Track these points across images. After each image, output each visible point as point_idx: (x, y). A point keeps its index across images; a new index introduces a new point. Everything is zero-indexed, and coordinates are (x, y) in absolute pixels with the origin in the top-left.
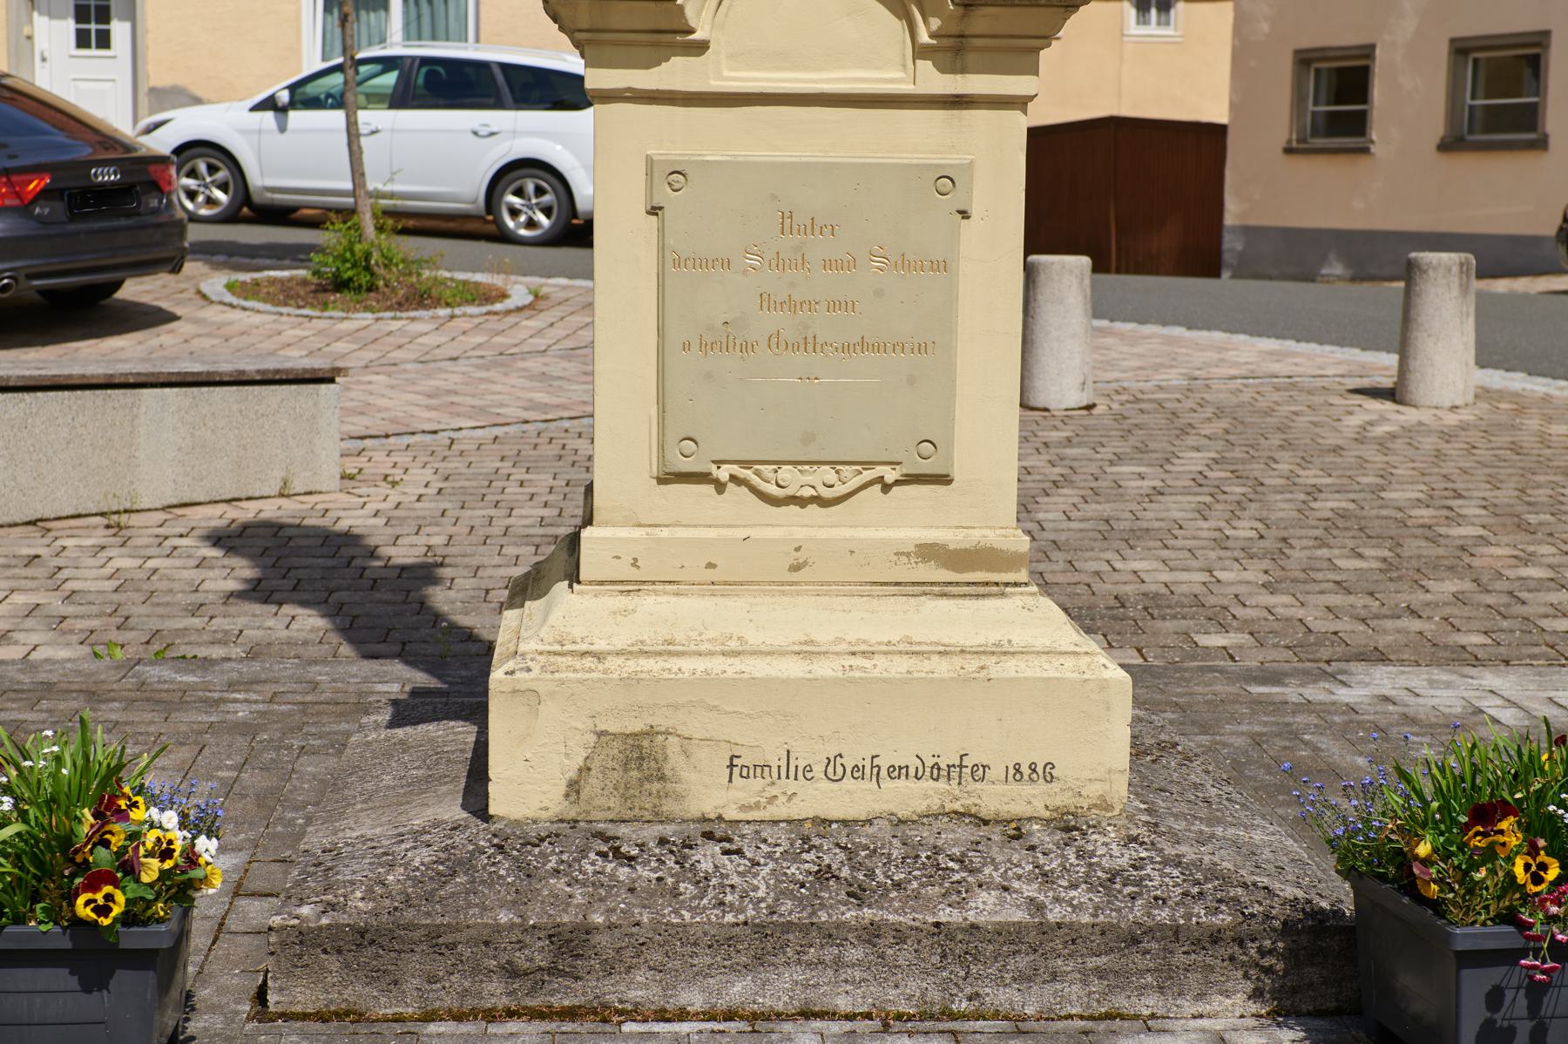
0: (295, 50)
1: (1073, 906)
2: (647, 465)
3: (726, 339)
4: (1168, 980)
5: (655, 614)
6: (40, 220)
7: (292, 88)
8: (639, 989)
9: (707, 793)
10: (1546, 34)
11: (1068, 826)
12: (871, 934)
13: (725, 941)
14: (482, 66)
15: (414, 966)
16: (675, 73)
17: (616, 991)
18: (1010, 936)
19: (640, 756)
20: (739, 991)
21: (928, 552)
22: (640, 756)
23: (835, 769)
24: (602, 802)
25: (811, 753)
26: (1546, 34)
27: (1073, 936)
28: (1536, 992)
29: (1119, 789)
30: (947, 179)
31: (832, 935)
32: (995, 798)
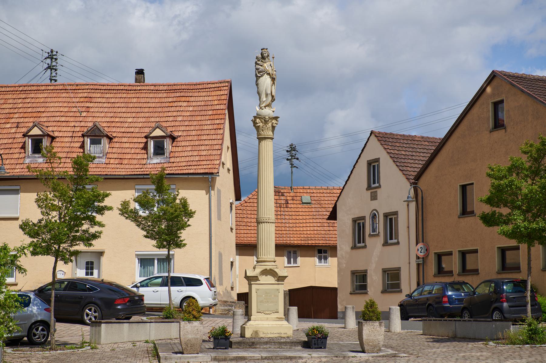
0: (134, 275)
1: (288, 340)
2: (256, 311)
3: (262, 302)
4: (295, 346)
5: (257, 322)
6: (128, 306)
7: (140, 283)
8: (258, 346)
9: (261, 335)
10: (400, 268)
11: (288, 337)
12: (274, 342)
13: (264, 343)
14: (180, 277)
15: (243, 344)
16: (258, 282)
17: (256, 346)
18: (284, 342)
19: (256, 332)
20: (265, 346)
21: (277, 318)
22: (256, 332)
23: (271, 333)
24: (254, 336)
25: (269, 332)
26: (400, 268)
27: (288, 342)
28: (317, 341)
29: (292, 335)
30: (278, 290)
31: (271, 342)
32: (282, 336)
